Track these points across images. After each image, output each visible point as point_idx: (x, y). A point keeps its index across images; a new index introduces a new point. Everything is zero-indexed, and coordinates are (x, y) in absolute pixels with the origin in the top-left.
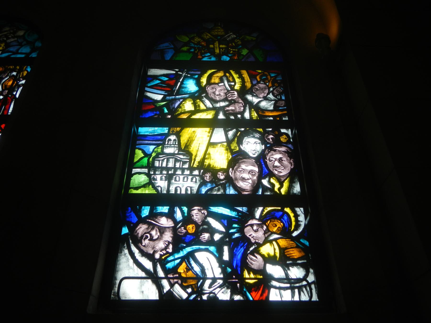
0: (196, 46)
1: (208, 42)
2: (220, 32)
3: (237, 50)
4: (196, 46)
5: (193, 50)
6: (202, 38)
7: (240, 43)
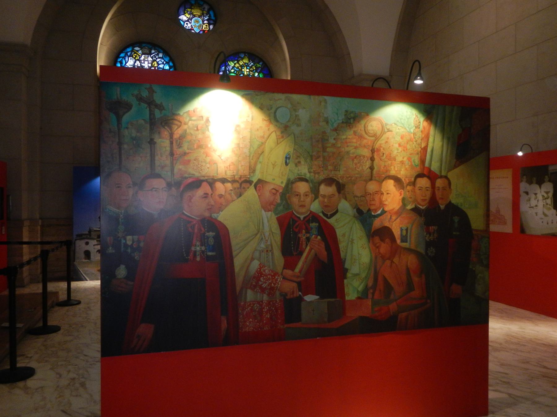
0: (237, 69)
1: (242, 66)
2: (246, 61)
3: (253, 73)
4: (237, 69)
5: (235, 72)
6: (239, 64)
7: (254, 69)
